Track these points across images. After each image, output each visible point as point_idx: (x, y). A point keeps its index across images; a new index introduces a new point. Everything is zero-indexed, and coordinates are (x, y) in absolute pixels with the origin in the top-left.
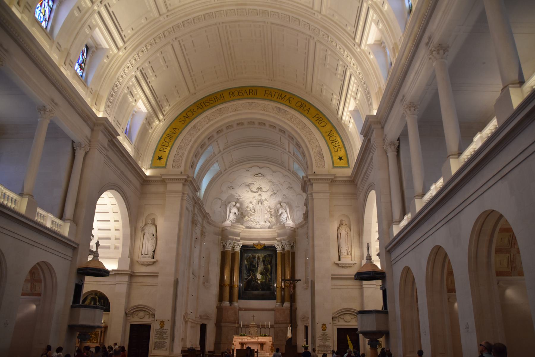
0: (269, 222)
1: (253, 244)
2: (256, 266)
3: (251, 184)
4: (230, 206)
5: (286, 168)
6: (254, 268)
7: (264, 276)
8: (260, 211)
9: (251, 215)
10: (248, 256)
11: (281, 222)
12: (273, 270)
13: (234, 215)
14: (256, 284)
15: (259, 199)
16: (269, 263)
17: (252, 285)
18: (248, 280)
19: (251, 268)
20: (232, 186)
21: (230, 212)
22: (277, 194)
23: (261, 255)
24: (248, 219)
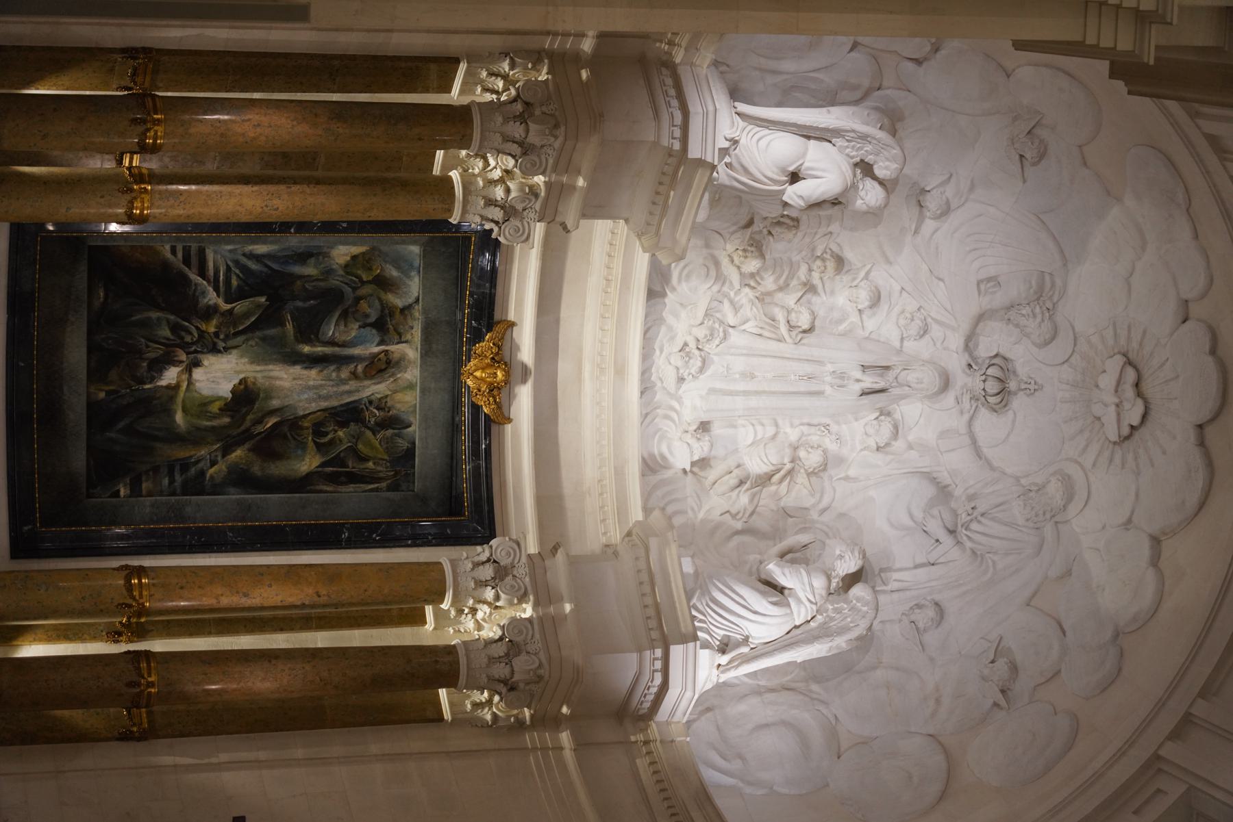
0: (702, 463)
1: (512, 316)
2: (306, 349)
3: (1051, 311)
4: (864, 137)
5: (1203, 694)
6: (289, 327)
7: (226, 420)
8: (803, 386)
9: (761, 299)
10: (398, 262)
11: (706, 592)
12: (274, 505)
13: (783, 170)
14: (152, 355)
15: (911, 377)
16: (338, 461)
17: (138, 317)
18: (186, 280)
19: (299, 304)
20: (1042, 156)
21: (809, 133)
22: (955, 553)
23: (411, 386)
24: (735, 277)
